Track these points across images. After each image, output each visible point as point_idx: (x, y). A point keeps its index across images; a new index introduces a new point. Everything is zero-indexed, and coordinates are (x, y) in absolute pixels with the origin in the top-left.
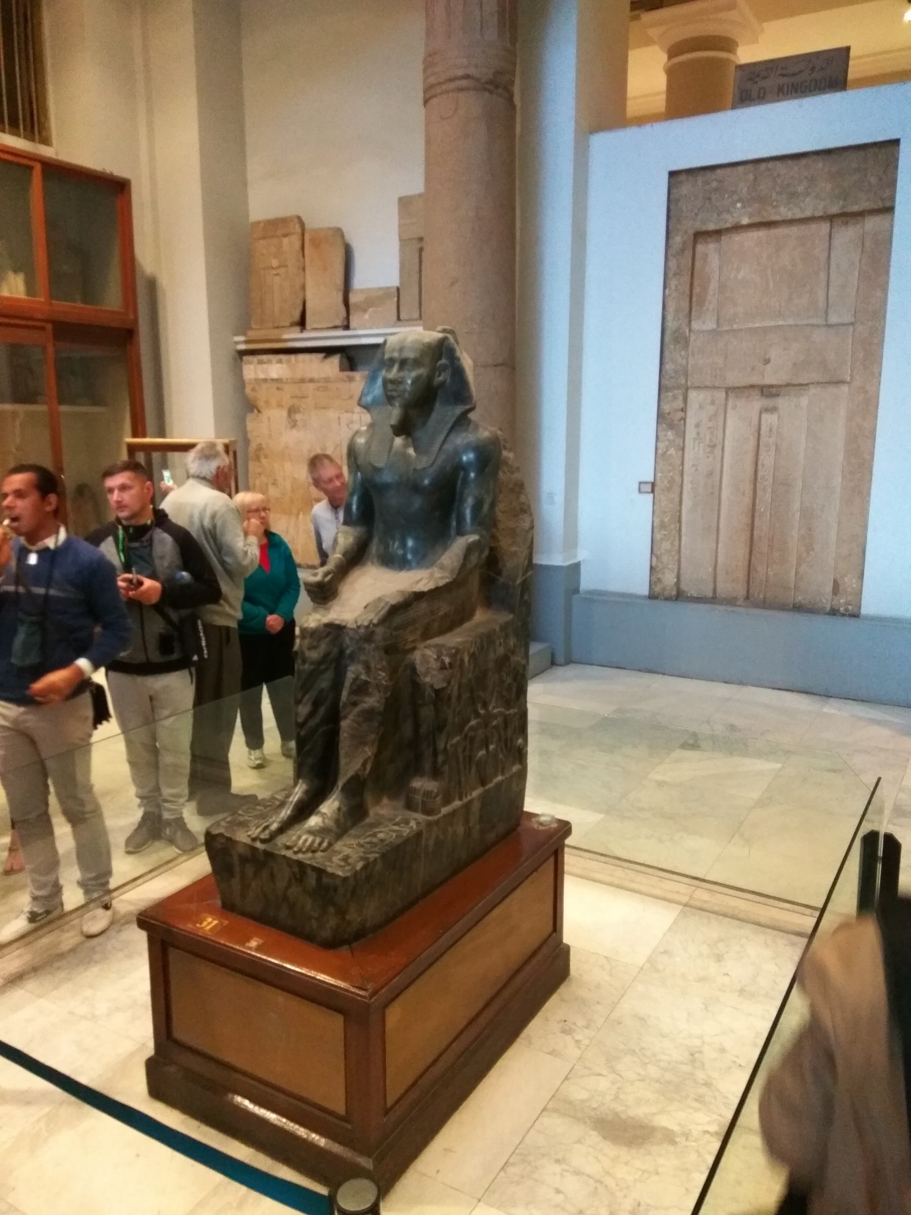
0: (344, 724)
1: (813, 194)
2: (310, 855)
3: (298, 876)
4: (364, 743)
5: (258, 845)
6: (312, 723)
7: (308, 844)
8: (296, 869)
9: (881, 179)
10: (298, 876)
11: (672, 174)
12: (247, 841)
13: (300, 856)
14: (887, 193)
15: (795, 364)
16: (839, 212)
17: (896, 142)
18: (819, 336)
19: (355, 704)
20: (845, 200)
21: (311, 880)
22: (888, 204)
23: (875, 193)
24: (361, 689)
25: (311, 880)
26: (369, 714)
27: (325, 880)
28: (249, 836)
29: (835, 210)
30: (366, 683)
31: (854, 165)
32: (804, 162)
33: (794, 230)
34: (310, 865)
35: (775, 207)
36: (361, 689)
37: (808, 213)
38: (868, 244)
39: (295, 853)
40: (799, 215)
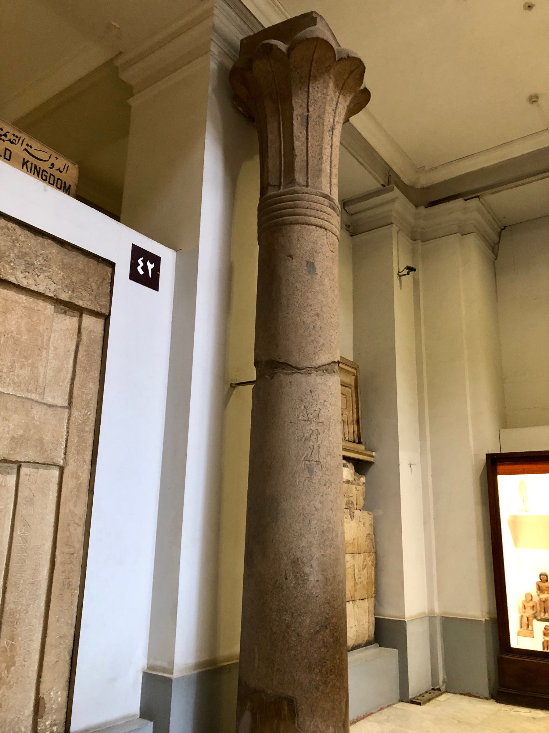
1: (46, 274)
9: (98, 288)
15: (13, 438)
16: (67, 299)
17: (112, 265)
18: (38, 412)
20: (73, 291)
22: (103, 311)
23: (95, 297)
29: (64, 297)
31: (81, 266)
32: (40, 239)
33: (23, 299)
35: (13, 268)
37: (41, 289)
38: (84, 337)
40: (33, 288)
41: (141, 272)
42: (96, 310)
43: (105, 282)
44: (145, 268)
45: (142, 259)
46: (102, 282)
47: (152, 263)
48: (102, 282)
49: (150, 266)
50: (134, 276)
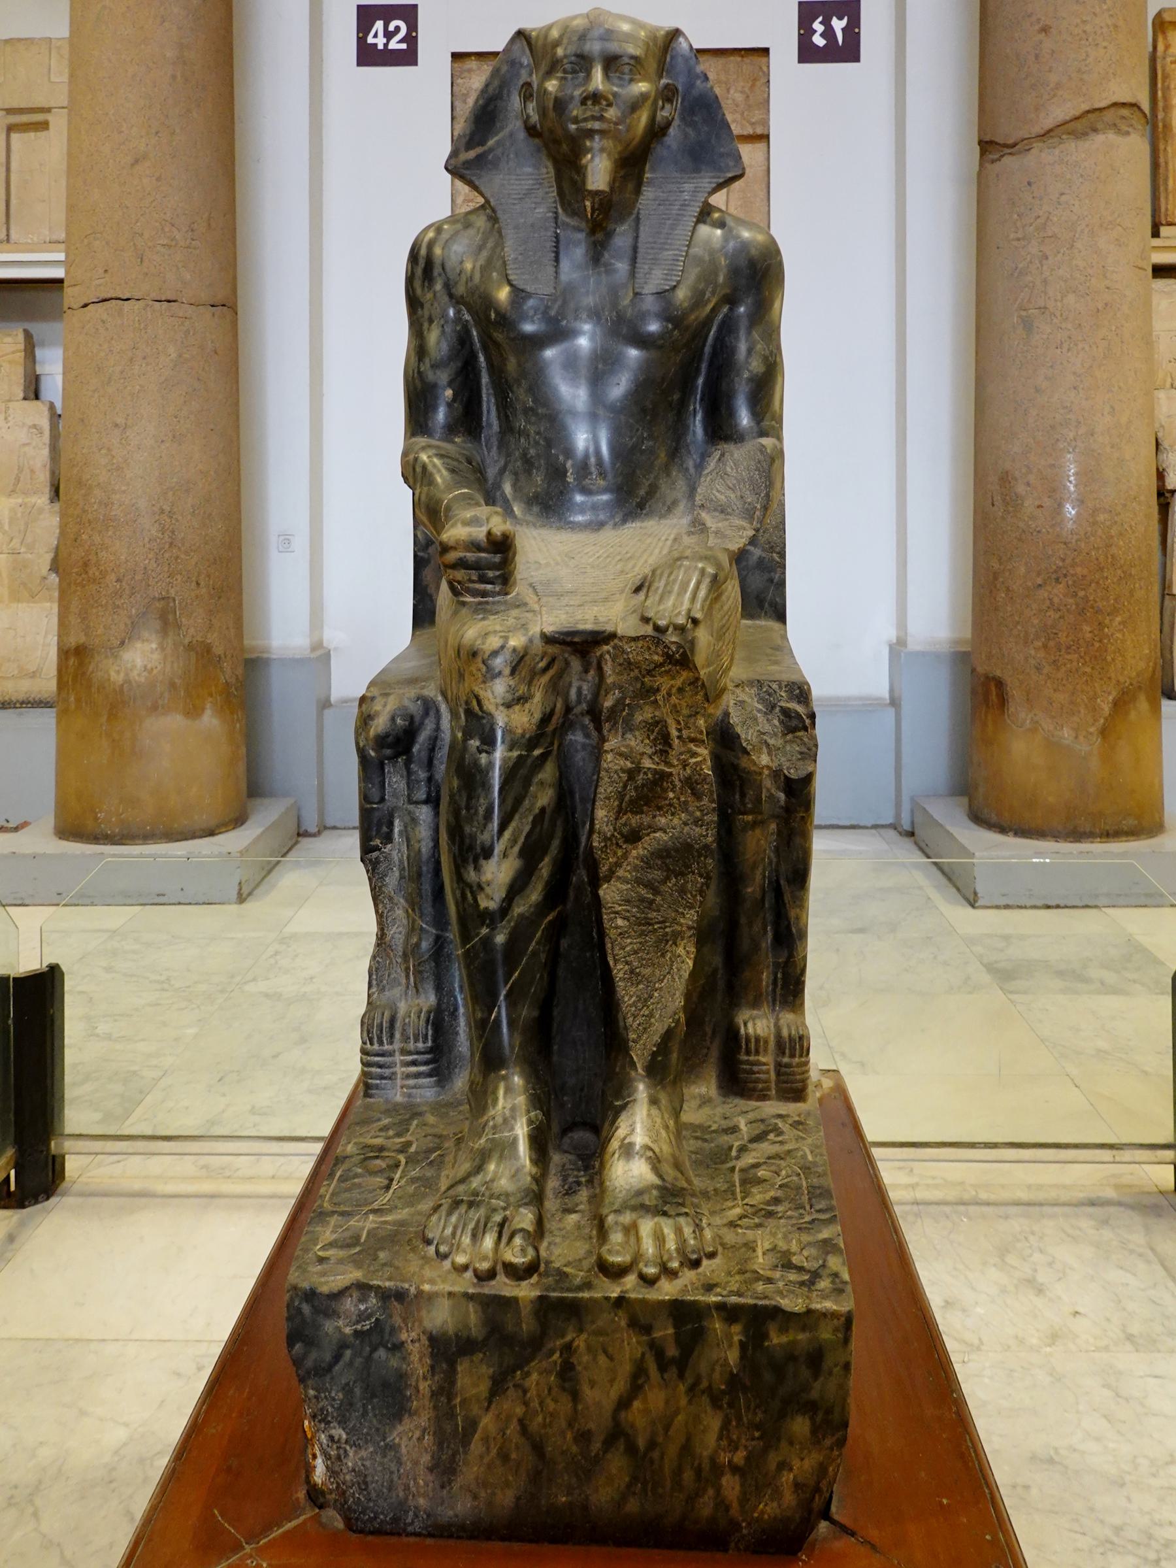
0: (609, 893)
2: (689, 1275)
3: (672, 1351)
4: (676, 937)
5: (503, 1286)
6: (520, 908)
7: (671, 1245)
8: (665, 1331)
10: (672, 1351)
11: (457, 57)
12: (466, 1284)
13: (667, 1290)
14: (757, 116)
17: (765, 51)
19: (634, 837)
21: (725, 1348)
22: (759, 131)
23: (742, 114)
24: (647, 794)
25: (725, 1348)
26: (676, 859)
27: (777, 1339)
28: (465, 1268)
30: (661, 778)
34: (721, 1307)
36: (647, 794)
39: (648, 1281)
41: (819, 41)
42: (745, 133)
43: (758, 84)
44: (829, 33)
45: (820, 19)
46: (753, 86)
47: (840, 18)
48: (753, 86)
49: (838, 25)
50: (807, 53)
